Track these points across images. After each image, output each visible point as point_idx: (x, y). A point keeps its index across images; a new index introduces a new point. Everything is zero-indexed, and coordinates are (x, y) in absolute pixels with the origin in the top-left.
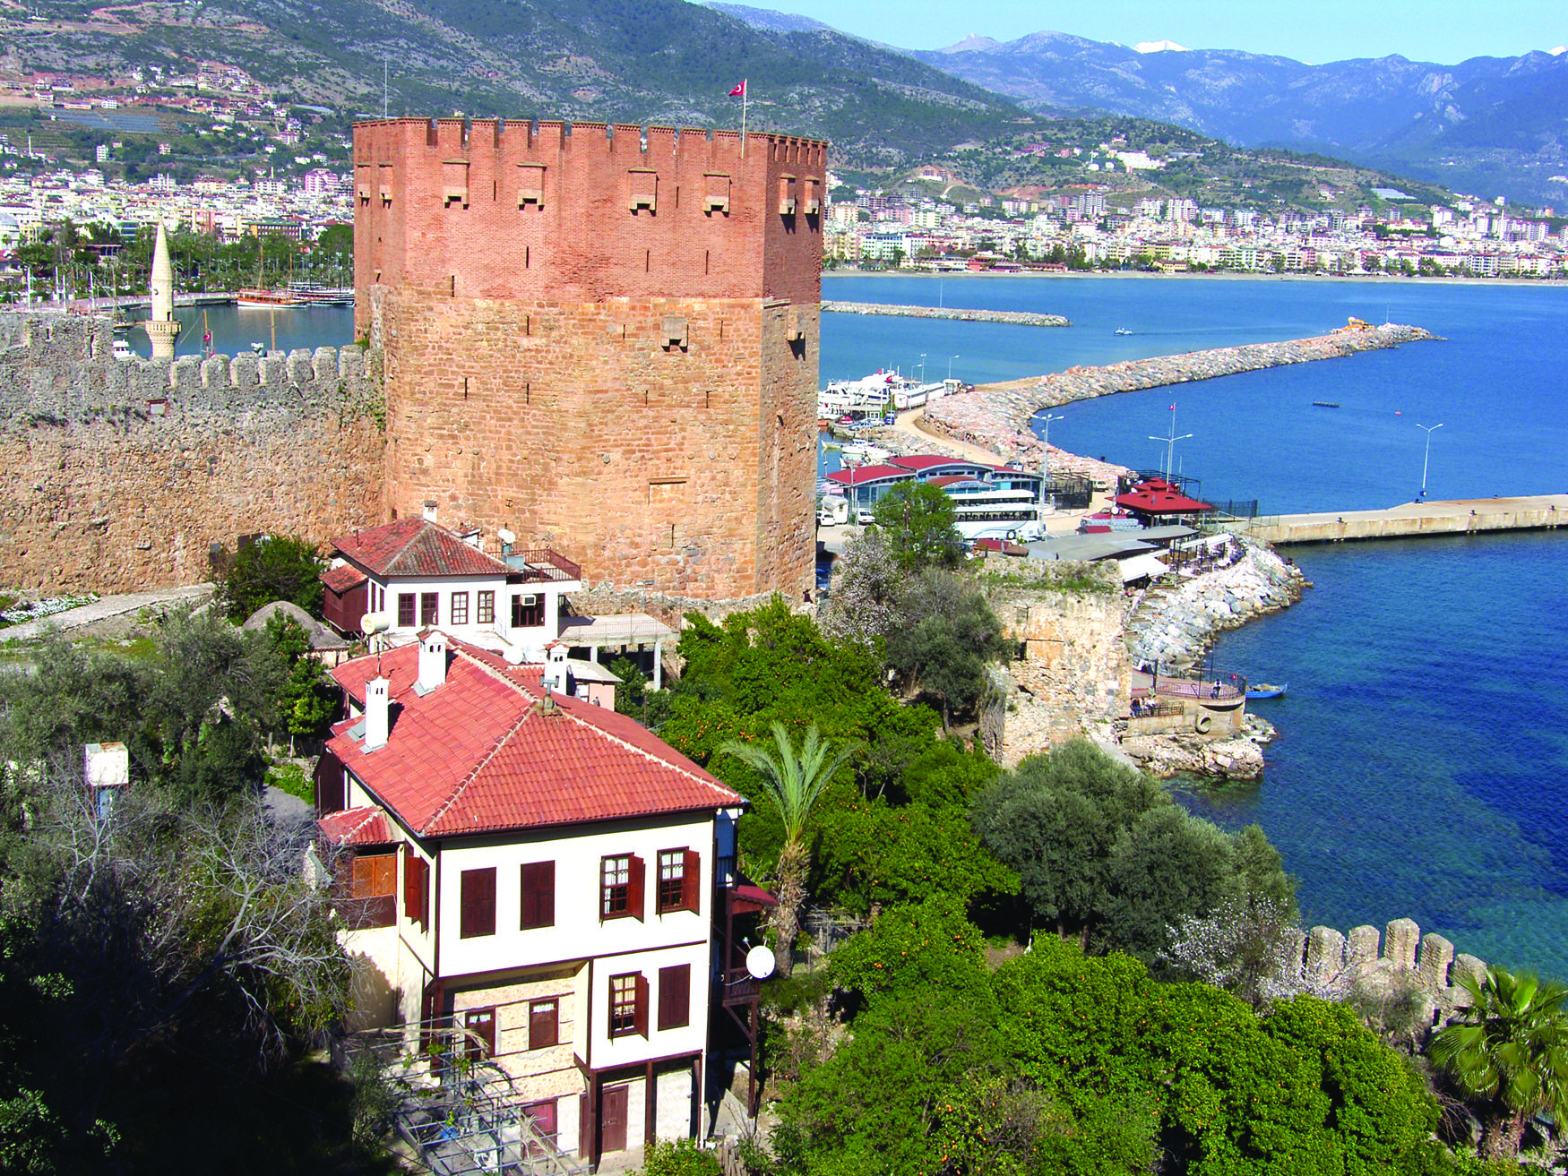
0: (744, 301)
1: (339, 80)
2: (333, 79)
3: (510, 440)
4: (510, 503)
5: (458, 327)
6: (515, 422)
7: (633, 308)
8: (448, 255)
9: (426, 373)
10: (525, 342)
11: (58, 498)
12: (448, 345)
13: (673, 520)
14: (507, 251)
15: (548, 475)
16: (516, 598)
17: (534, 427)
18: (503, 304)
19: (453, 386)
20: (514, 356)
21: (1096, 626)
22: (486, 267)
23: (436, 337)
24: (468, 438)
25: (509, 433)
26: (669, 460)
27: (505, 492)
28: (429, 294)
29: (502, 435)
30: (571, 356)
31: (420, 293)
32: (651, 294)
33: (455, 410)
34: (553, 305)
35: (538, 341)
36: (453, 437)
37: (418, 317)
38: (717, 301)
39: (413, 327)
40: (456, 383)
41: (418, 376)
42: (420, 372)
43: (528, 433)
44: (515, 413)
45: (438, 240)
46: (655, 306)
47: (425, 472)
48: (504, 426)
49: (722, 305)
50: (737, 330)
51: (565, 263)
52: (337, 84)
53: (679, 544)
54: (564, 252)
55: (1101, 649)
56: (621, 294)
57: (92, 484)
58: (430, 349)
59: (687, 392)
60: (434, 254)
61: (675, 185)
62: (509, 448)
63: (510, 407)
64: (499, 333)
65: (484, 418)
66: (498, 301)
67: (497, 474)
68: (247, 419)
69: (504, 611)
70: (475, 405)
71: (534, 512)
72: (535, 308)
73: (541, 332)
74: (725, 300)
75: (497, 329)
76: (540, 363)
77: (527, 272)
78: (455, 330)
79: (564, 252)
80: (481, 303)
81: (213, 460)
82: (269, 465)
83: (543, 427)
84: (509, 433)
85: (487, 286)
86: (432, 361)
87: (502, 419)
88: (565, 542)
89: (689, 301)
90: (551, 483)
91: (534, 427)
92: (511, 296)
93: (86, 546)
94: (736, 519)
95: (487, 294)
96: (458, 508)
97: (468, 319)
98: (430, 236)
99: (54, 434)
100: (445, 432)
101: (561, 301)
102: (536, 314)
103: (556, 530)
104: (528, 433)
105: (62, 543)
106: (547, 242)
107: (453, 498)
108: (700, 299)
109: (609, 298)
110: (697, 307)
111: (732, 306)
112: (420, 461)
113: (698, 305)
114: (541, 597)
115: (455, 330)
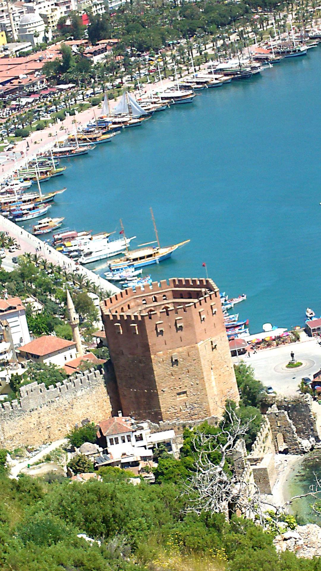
0: (193, 346)
7: (164, 354)
13: (185, 401)
16: (135, 436)
19: (127, 376)
26: (180, 388)
34: (145, 356)
38: (185, 347)
47: (125, 396)
49: (187, 348)
53: (188, 407)
57: (45, 419)
59: (183, 370)
68: (79, 393)
69: (133, 439)
74: (188, 347)
80: (129, 356)
81: (72, 406)
89: (178, 349)
93: (47, 433)
95: (130, 354)
99: (35, 412)
110: (181, 350)
111: (190, 347)
113: (180, 349)
114: (141, 434)
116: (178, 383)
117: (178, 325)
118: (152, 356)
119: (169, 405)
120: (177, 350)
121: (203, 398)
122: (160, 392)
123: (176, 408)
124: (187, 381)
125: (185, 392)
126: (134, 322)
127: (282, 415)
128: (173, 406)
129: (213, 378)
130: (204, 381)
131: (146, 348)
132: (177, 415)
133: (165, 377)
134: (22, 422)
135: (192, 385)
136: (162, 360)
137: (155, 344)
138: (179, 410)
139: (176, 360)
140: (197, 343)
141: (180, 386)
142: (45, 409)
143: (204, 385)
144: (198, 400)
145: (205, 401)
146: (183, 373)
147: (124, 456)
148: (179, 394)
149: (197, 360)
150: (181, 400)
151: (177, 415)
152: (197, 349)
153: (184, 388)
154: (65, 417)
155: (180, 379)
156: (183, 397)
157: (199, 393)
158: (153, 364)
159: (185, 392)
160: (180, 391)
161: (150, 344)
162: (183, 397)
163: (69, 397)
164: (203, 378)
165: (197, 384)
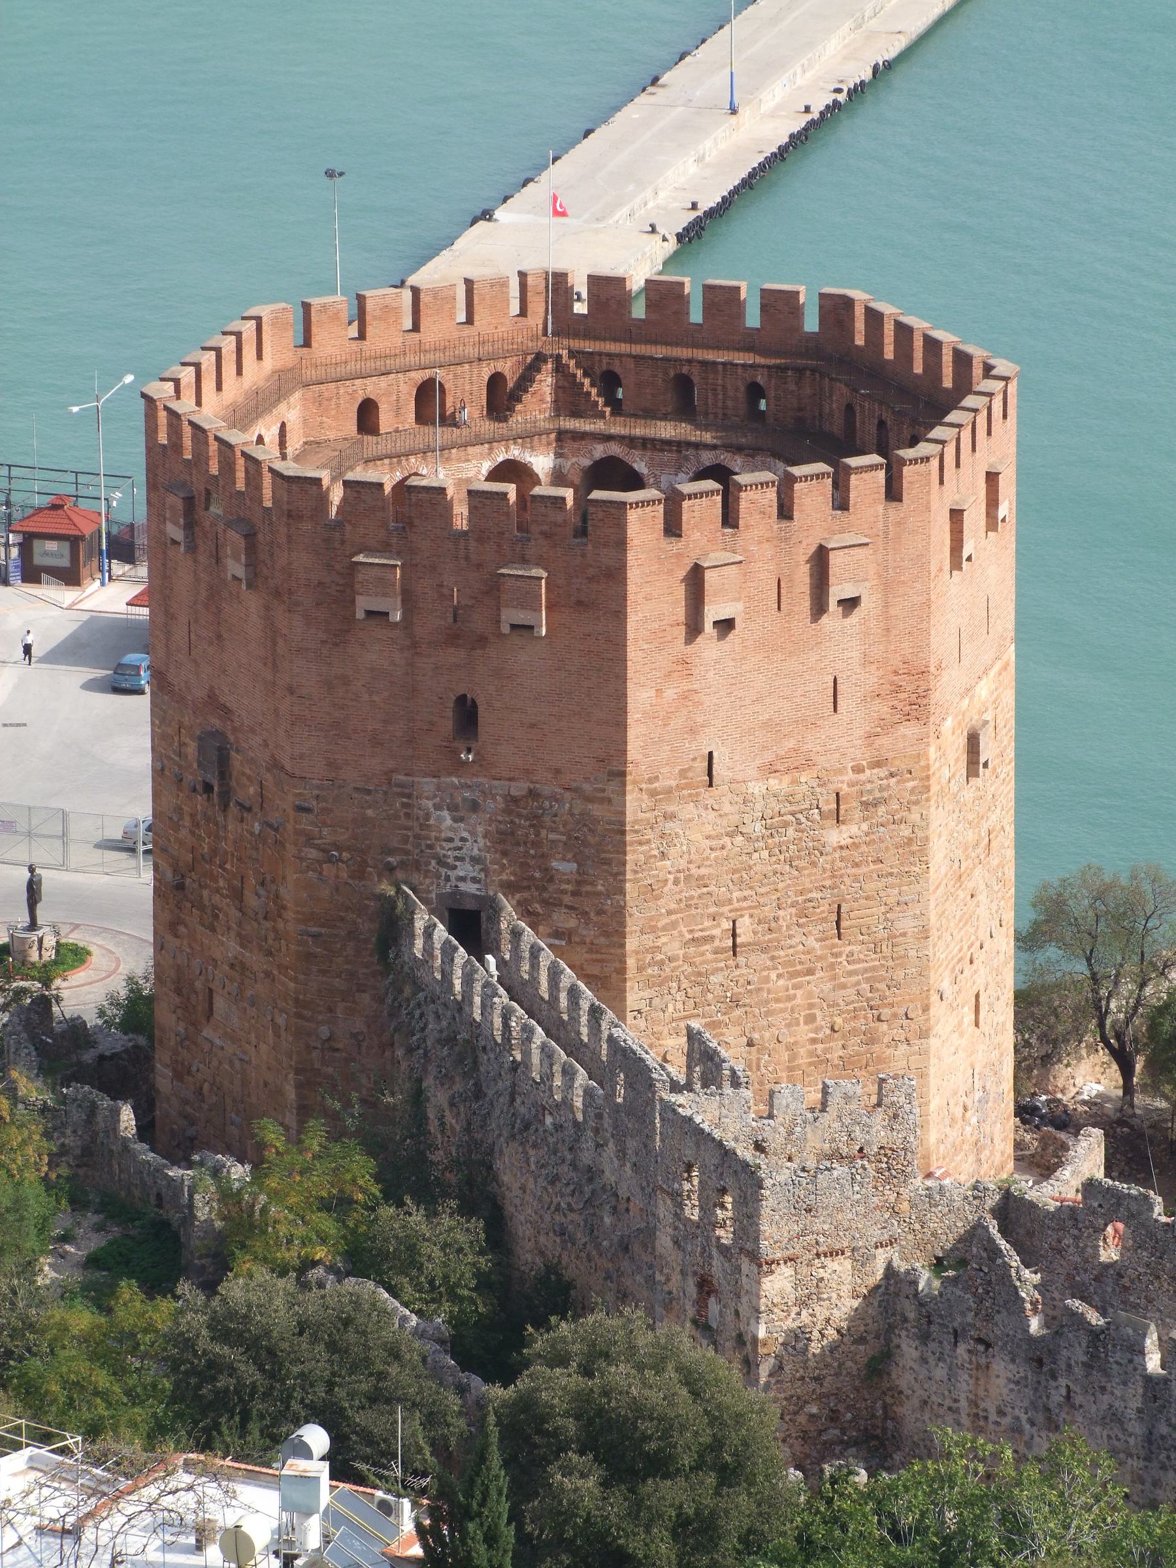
3: (811, 1006)
5: (719, 837)
6: (819, 974)
8: (700, 719)
9: (664, 928)
10: (835, 836)
12: (703, 871)
14: (800, 692)
15: (876, 1048)
17: (851, 973)
18: (796, 782)
19: (712, 938)
20: (814, 864)
22: (767, 725)
23: (683, 863)
25: (810, 995)
28: (669, 791)
29: (798, 1001)
31: (653, 793)
34: (878, 764)
35: (854, 829)
37: (649, 835)
40: (716, 932)
41: (651, 936)
42: (654, 929)
44: (820, 958)
45: (685, 696)
48: (795, 987)
54: (896, 673)
58: (670, 882)
60: (678, 722)
62: (811, 1019)
64: (791, 831)
65: (767, 979)
66: (787, 779)
67: (791, 1069)
70: (752, 962)
72: (850, 776)
73: (857, 814)
75: (786, 825)
76: (856, 865)
77: (836, 717)
78: (714, 843)
79: (896, 673)
83: (866, 970)
84: (810, 995)
85: (769, 756)
86: (673, 906)
87: (793, 975)
91: (851, 973)
92: (809, 763)
95: (771, 770)
97: (735, 819)
101: (890, 755)
102: (851, 784)
104: (844, 986)
106: (866, 661)
115: (714, 843)
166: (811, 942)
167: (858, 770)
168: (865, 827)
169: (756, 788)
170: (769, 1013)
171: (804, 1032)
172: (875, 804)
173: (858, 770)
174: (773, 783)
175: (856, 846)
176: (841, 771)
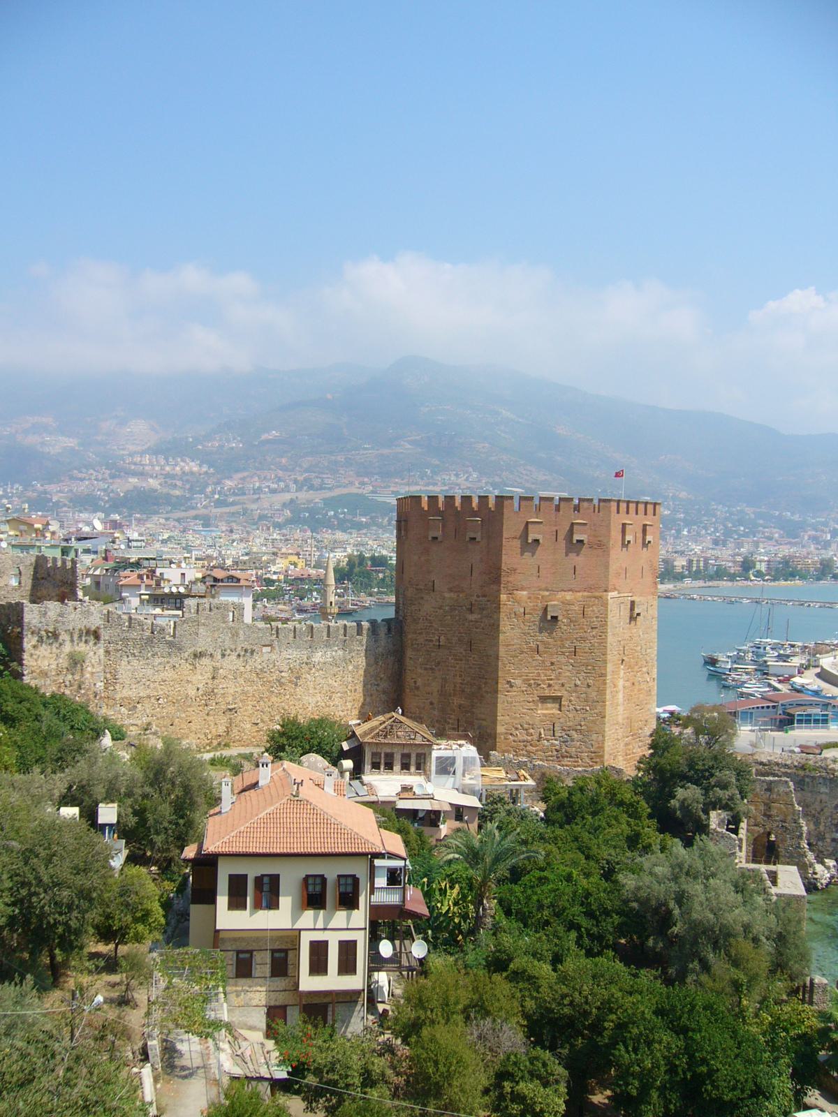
0: (597, 594)
1: (529, 473)
2: (524, 472)
4: (460, 706)
7: (529, 598)
10: (472, 617)
11: (211, 693)
18: (458, 596)
19: (432, 641)
20: (464, 624)
21: (824, 797)
23: (425, 614)
24: (439, 670)
25: (461, 668)
26: (550, 686)
27: (456, 701)
30: (493, 625)
32: (540, 590)
33: (433, 654)
34: (484, 596)
36: (432, 669)
38: (581, 594)
39: (413, 608)
43: (470, 668)
46: (543, 597)
47: (417, 688)
50: (593, 611)
51: (491, 573)
52: (527, 475)
55: (827, 812)
56: (522, 589)
57: (230, 689)
59: (564, 647)
61: (554, 529)
62: (461, 676)
63: (461, 653)
68: (318, 657)
71: (473, 713)
72: (475, 598)
74: (586, 594)
75: (455, 609)
76: (477, 628)
80: (447, 595)
81: (298, 678)
82: (330, 682)
87: (456, 660)
88: (488, 731)
89: (563, 593)
90: (482, 696)
92: (463, 592)
93: (223, 721)
94: (593, 721)
95: (450, 590)
96: (434, 709)
98: (422, 559)
99: (205, 661)
100: (428, 666)
102: (476, 601)
103: (484, 723)
104: (470, 668)
105: (211, 718)
107: (431, 703)
108: (571, 593)
109: (515, 592)
111: (588, 597)
112: (415, 682)
113: (569, 596)
116: (549, 673)
117: (576, 537)
118: (503, 597)
119: (517, 722)
120: (560, 595)
121: (594, 722)
122: (502, 685)
123: (532, 731)
124: (568, 674)
125: (557, 700)
126: (475, 514)
127: (782, 789)
128: (526, 726)
129: (621, 683)
130: (605, 684)
131: (494, 575)
132: (529, 748)
133: (522, 652)
134: (169, 674)
135: (576, 685)
136: (522, 610)
137: (515, 570)
138: (535, 737)
139: (555, 618)
140: (606, 591)
141: (551, 682)
142: (232, 662)
143: (602, 692)
144: (583, 723)
145: (596, 728)
146: (563, 653)
147: (406, 795)
148: (544, 699)
149: (601, 626)
150: (545, 715)
151: (529, 748)
152: (605, 605)
153: (556, 688)
154: (274, 699)
155: (552, 664)
156: (551, 709)
157: (588, 708)
158: (502, 615)
159: (557, 700)
160: (547, 693)
161: (504, 567)
162: (552, 708)
163: (294, 655)
164: (604, 675)
165: (589, 686)
166: (462, 650)
167: (478, 596)
168: (479, 616)
169: (447, 595)
170: (448, 670)
171: (459, 680)
172: (483, 609)
173: (478, 596)
174: (452, 594)
175: (477, 622)
176: (473, 596)
